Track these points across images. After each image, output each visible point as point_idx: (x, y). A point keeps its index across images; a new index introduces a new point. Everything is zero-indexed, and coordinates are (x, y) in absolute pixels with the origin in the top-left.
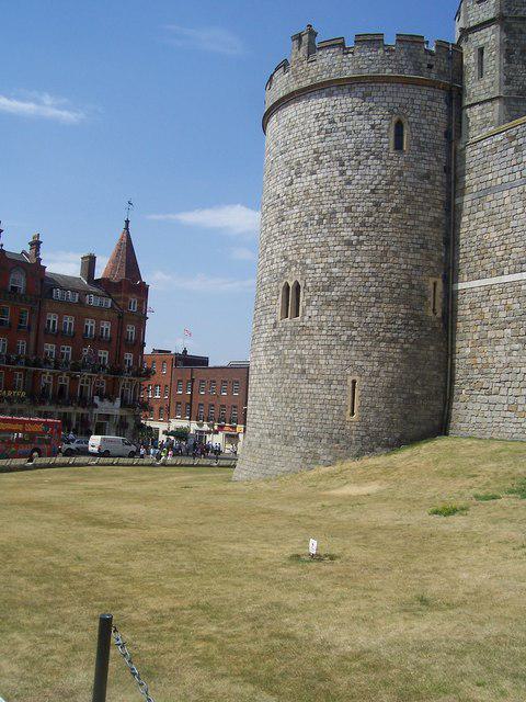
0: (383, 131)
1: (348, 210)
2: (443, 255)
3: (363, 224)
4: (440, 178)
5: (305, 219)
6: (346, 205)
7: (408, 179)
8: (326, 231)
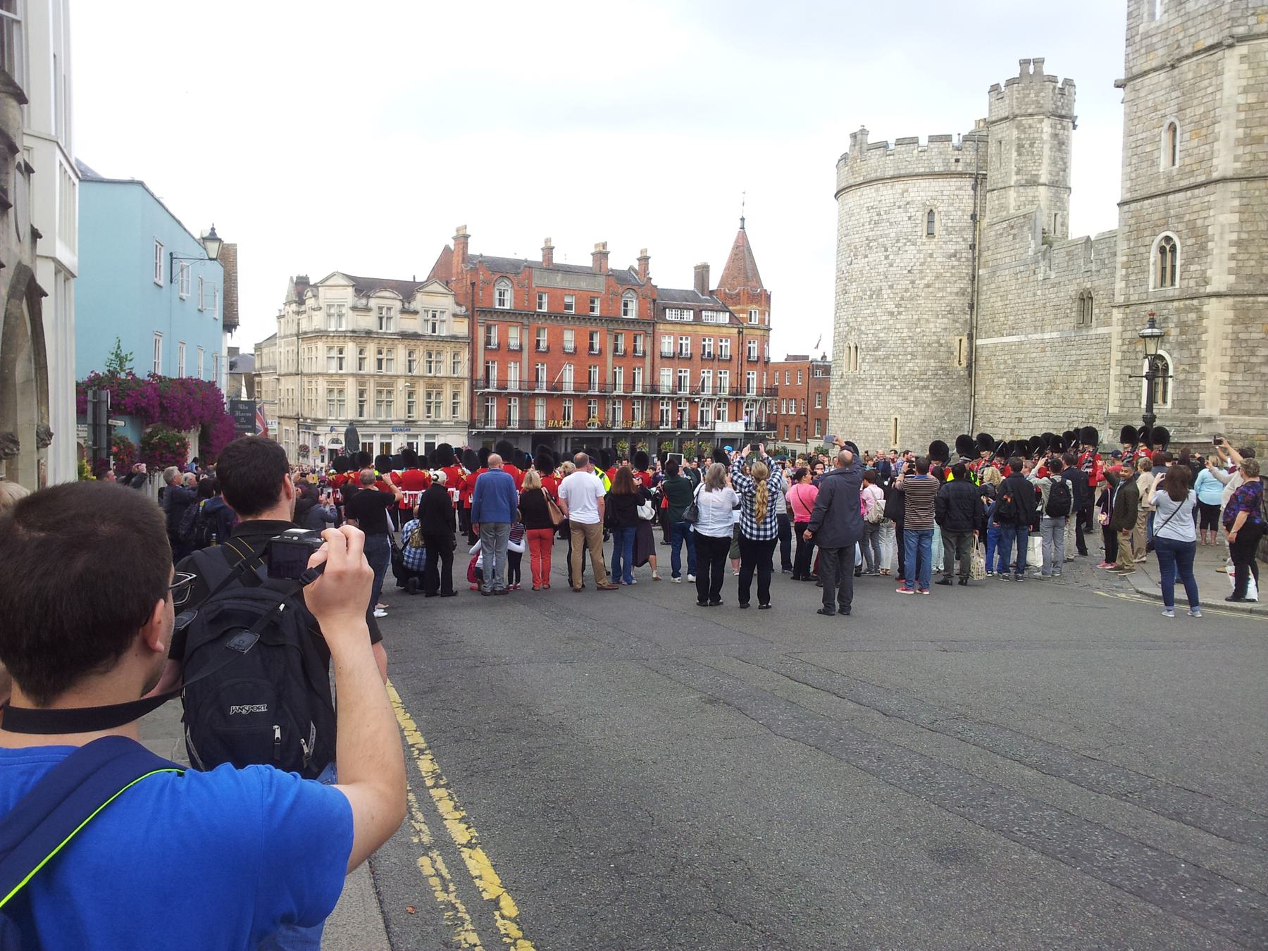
0: (917, 222)
1: (891, 287)
2: (968, 317)
3: (902, 299)
4: (967, 254)
5: (861, 294)
6: (890, 283)
7: (938, 260)
8: (875, 304)
